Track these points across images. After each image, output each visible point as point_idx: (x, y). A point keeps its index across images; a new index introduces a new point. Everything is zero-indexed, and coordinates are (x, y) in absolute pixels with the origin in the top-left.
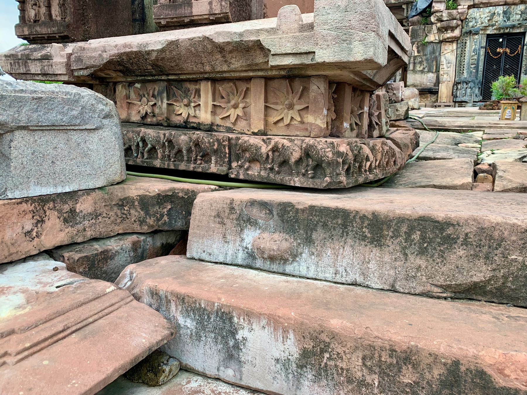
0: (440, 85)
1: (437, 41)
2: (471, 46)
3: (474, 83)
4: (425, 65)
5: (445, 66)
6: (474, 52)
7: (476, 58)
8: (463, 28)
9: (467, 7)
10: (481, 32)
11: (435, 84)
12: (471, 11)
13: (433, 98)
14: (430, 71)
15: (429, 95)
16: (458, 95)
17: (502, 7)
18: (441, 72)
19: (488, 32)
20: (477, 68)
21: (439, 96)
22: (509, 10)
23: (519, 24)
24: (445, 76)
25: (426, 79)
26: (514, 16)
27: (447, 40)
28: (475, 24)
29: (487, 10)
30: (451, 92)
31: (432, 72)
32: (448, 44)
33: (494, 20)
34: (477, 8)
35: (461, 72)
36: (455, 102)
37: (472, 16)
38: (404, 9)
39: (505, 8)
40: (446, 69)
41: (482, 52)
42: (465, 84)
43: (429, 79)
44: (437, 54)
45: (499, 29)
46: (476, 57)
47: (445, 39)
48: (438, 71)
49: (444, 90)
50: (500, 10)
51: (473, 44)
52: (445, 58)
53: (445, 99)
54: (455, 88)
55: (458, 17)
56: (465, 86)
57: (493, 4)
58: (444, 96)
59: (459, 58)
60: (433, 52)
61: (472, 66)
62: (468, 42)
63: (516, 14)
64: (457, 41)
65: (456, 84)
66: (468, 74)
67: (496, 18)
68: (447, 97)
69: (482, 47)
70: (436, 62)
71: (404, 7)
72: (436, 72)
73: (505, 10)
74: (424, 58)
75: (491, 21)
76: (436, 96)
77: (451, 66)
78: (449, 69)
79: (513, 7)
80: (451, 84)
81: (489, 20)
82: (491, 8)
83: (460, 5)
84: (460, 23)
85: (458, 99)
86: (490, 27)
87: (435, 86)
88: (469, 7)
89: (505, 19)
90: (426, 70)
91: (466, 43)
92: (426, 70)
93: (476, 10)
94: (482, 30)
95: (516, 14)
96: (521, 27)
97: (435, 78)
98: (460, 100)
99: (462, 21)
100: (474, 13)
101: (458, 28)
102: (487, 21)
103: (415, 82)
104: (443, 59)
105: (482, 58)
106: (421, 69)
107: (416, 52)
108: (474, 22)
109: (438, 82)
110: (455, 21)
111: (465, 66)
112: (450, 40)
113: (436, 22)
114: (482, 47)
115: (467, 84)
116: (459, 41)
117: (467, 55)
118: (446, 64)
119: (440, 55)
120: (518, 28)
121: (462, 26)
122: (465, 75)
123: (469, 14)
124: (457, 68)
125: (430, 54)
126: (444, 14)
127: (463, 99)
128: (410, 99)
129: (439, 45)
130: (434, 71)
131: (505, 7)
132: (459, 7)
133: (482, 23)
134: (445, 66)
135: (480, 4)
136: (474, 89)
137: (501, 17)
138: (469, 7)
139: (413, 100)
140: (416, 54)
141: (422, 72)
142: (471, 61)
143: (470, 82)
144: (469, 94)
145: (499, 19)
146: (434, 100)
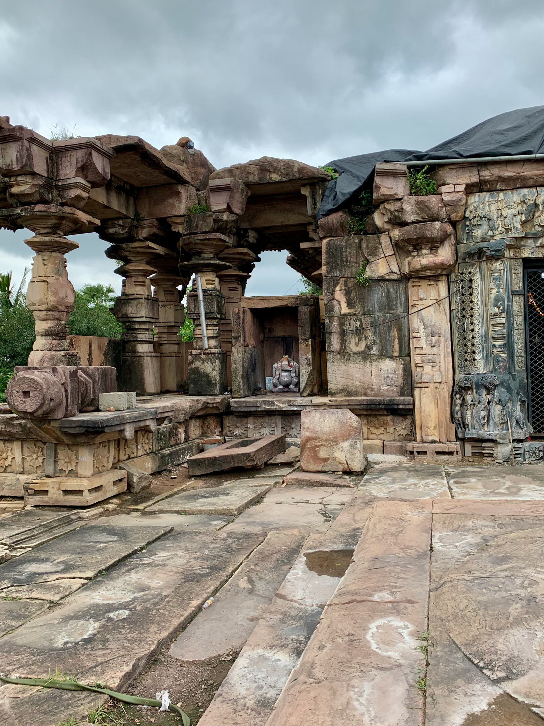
0: (417, 392)
1: (395, 277)
2: (486, 291)
3: (509, 390)
4: (370, 337)
5: (423, 342)
6: (496, 306)
7: (504, 321)
8: (458, 242)
9: (462, 188)
10: (507, 254)
11: (402, 388)
12: (474, 199)
13: (401, 427)
14: (384, 354)
15: (389, 418)
16: (469, 420)
18: (416, 359)
19: (526, 253)
20: (509, 347)
21: (417, 423)
24: (428, 368)
25: (378, 376)
27: (422, 274)
28: (490, 233)
29: (515, 197)
30: (448, 412)
31: (392, 358)
32: (424, 283)
34: (488, 191)
35: (469, 358)
36: (463, 440)
37: (480, 212)
38: (305, 197)
40: (426, 349)
41: (517, 305)
42: (484, 392)
43: (384, 374)
44: (400, 310)
46: (503, 320)
47: (417, 271)
48: (405, 354)
49: (430, 408)
51: (492, 285)
52: (422, 321)
53: (436, 432)
54: (459, 402)
55: (443, 213)
56: (485, 397)
57: (531, 182)
58: (432, 422)
59: (456, 322)
60: (389, 305)
61: (497, 343)
62: (477, 278)
64: (448, 276)
65: (459, 390)
66: (487, 363)
68: (439, 426)
69: (514, 293)
70: (400, 330)
71: (305, 192)
72: (400, 356)
74: (366, 320)
75: (529, 225)
76: (409, 421)
77: (439, 341)
78: (435, 350)
80: (445, 391)
82: (525, 191)
83: (444, 184)
84: (449, 228)
85: (471, 434)
86: (530, 241)
87: (402, 394)
88: (470, 189)
90: (375, 350)
91: (471, 281)
92: (375, 350)
93: (486, 196)
94: (509, 247)
97: (401, 372)
98: (475, 437)
99: (454, 224)
100: (482, 204)
101: (447, 244)
103: (350, 382)
104: (415, 322)
105: (519, 320)
106: (362, 347)
107: (344, 305)
108: (485, 227)
109: (409, 385)
110: (437, 225)
111: (477, 342)
112: (429, 273)
113: (387, 226)
114: (514, 293)
115: (489, 391)
116: (453, 277)
117: (478, 312)
118: (427, 336)
119: (406, 311)
121: (456, 237)
122: (481, 366)
123: (471, 208)
124: (456, 348)
125: (380, 310)
126: (407, 207)
127: (486, 432)
128: (336, 441)
129: (402, 287)
130: (396, 354)
132: (444, 189)
133: (508, 230)
134: (423, 342)
135: (497, 182)
136: (509, 405)
139: (346, 445)
140: (345, 310)
141: (365, 356)
142: (491, 328)
143: (496, 386)
144: (497, 420)
146: (403, 432)
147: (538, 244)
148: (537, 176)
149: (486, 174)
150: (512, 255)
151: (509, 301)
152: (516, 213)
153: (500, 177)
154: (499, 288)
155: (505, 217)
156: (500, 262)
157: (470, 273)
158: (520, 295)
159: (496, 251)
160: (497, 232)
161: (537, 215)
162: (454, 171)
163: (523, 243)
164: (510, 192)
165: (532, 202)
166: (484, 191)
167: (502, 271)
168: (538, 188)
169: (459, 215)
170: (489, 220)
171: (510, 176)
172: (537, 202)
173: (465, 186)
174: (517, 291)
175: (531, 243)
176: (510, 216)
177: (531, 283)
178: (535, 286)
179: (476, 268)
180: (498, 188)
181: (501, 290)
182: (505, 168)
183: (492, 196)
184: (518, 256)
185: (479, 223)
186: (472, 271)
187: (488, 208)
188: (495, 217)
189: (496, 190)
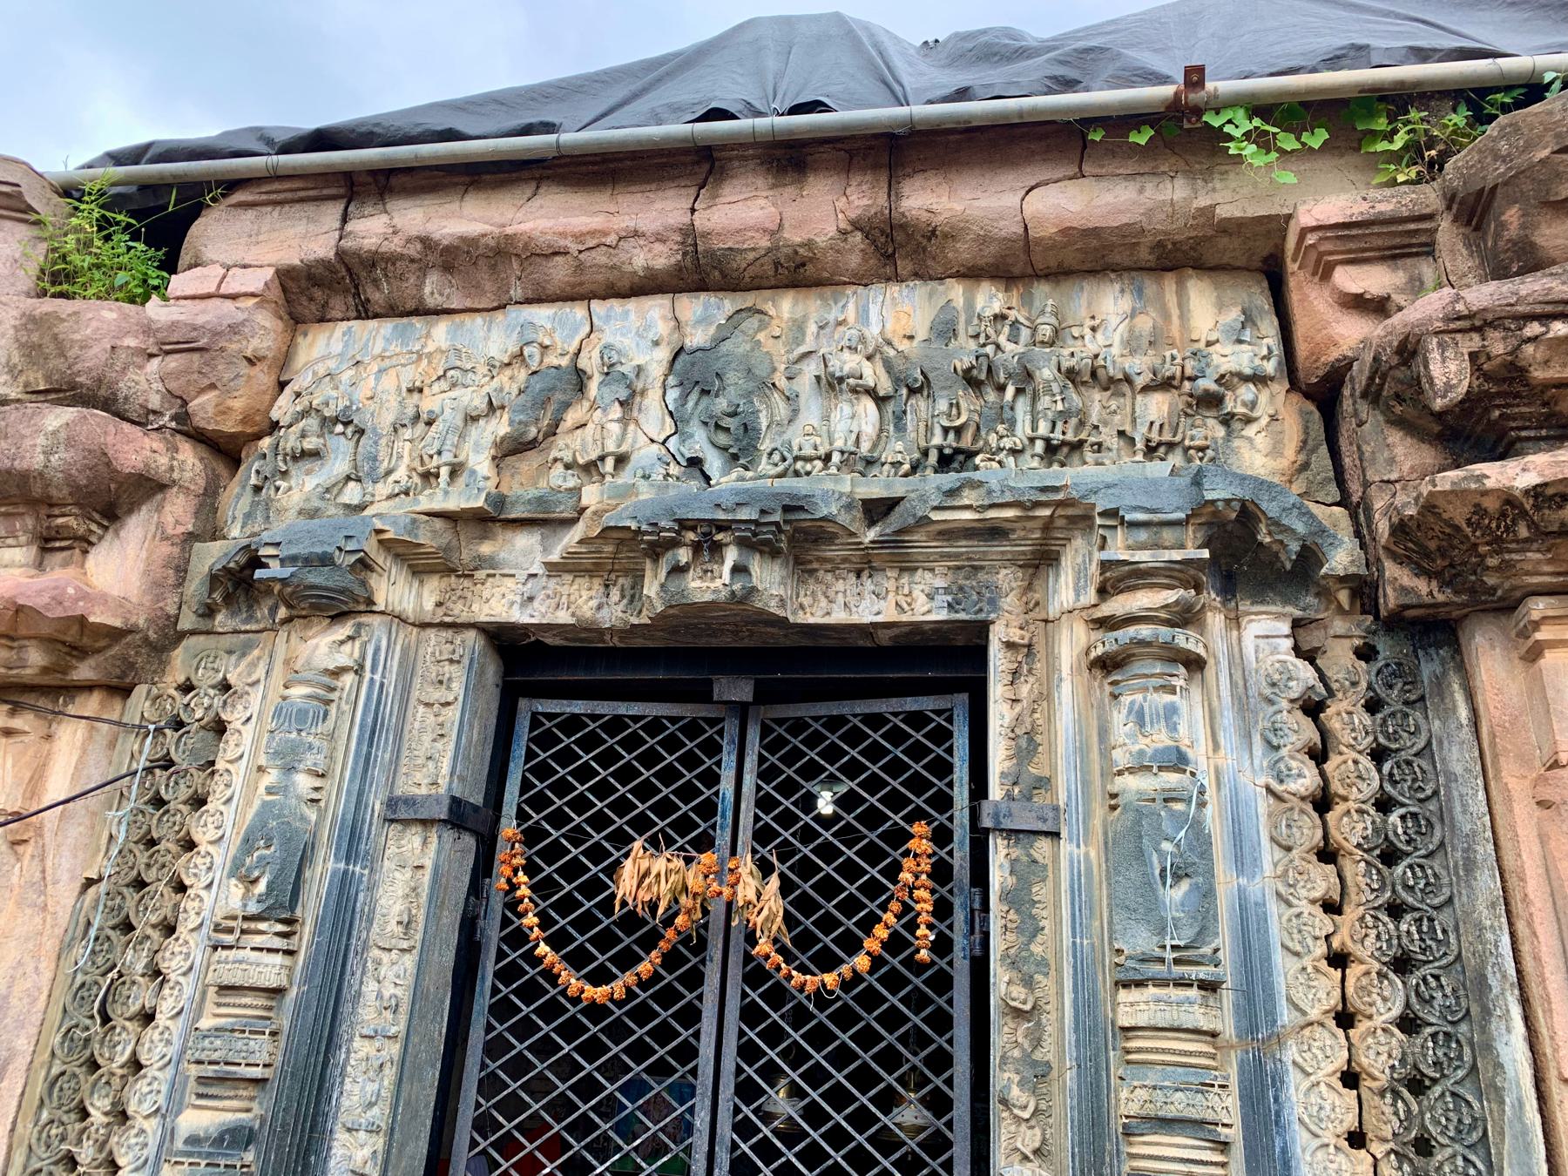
10: (394, 590)
17: (655, 309)
22: (737, 346)
23: (877, 510)
26: (811, 413)
29: (492, 337)
33: (568, 445)
34: (394, 311)
37: (331, 398)
39: (701, 316)
41: (408, 880)
45: (624, 551)
50: (639, 333)
57: (559, 272)
63: (832, 384)
67: (592, 429)
69: (401, 813)
73: (697, 338)
75: (527, 464)
79: (785, 306)
81: (512, 449)
82: (542, 314)
86: (525, 541)
88: (310, 294)
89: (699, 442)
91: (219, 728)
93: (377, 334)
94: (417, 562)
95: (832, 384)
96: (895, 555)
100: (349, 361)
102: (481, 463)
105: (392, 981)
114: (401, 813)
120: (865, 565)
131: (692, 306)
137: (653, 418)
138: (310, 294)
145: (638, 455)
147: (555, 557)
148: (579, 237)
149: (373, 229)
150: (429, 605)
151: (350, 855)
152: (480, 403)
153: (426, 242)
154: (290, 769)
155: (429, 423)
156: (345, 630)
157: (225, 687)
158: (426, 823)
159: (309, 561)
160: (383, 489)
161: (571, 417)
162: (251, 214)
163: (486, 548)
165: (564, 362)
166: (376, 316)
167: (348, 679)
168: (595, 304)
169: (238, 404)
170: (361, 432)
171: (463, 239)
172: (583, 363)
173: (270, 272)
174: (410, 802)
175: (527, 553)
176: (450, 418)
177: (542, 771)
178: (562, 788)
179: (253, 665)
180: (431, 302)
181: (303, 782)
182: (455, 206)
183: (402, 335)
184: (460, 612)
185: (310, 443)
187: (371, 381)
188: (387, 419)
189: (421, 311)
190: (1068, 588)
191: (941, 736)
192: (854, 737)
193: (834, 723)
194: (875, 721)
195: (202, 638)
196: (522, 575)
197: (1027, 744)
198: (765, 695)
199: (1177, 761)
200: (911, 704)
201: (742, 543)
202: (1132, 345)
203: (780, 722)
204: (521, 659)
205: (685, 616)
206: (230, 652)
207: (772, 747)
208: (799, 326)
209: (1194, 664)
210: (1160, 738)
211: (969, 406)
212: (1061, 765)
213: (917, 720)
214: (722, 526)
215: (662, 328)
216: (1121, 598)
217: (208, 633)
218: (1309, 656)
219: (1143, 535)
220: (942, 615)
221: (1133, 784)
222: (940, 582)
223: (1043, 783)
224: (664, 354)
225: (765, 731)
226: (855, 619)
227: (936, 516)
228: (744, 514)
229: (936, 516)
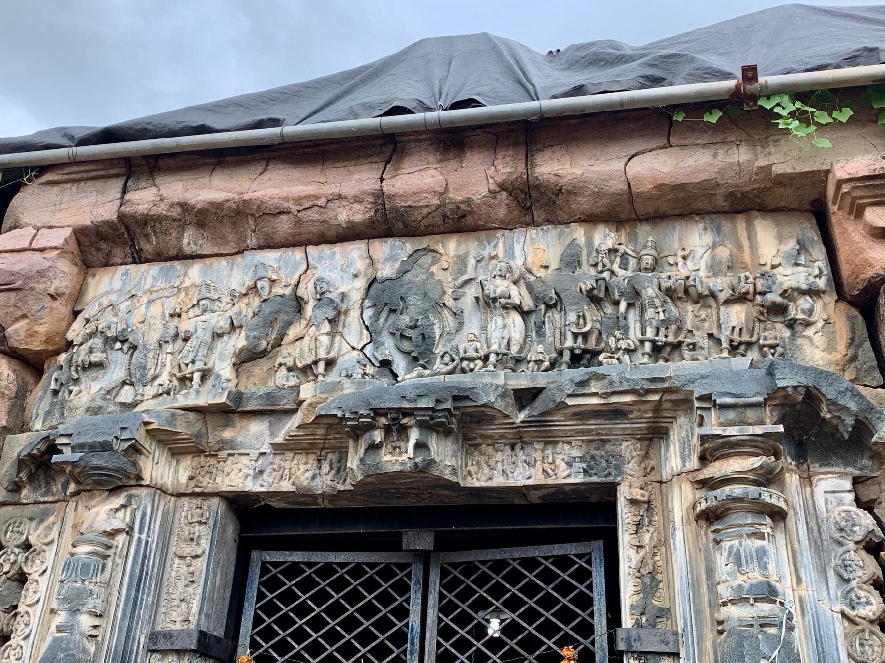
10: (158, 468)
12: (107, 284)
17: (355, 251)
19: (237, 476)
22: (416, 276)
23: (525, 397)
26: (472, 325)
29: (234, 275)
33: (289, 353)
34: (160, 257)
37: (112, 323)
39: (388, 255)
45: (331, 434)
50: (343, 269)
57: (283, 226)
63: (487, 303)
67: (307, 341)
73: (386, 271)
75: (259, 368)
79: (451, 247)
81: (247, 358)
82: (271, 257)
88: (97, 247)
89: (389, 349)
91: (22, 579)
94: (174, 445)
95: (487, 303)
96: (541, 432)
100: (126, 294)
102: (224, 369)
120: (517, 440)
131: (381, 248)
135: (181, 225)
137: (354, 331)
138: (97, 247)
145: (342, 359)
147: (279, 439)
148: (298, 201)
149: (145, 198)
150: (183, 478)
152: (224, 324)
153: (185, 207)
154: (74, 612)
155: (186, 340)
156: (118, 501)
157: (27, 546)
158: (180, 653)
160: (150, 391)
161: (293, 332)
162: (56, 189)
163: (227, 434)
164: (223, 263)
165: (287, 291)
166: (147, 261)
167: (121, 539)
168: (311, 249)
169: (42, 329)
170: (134, 348)
171: (212, 204)
172: (301, 292)
173: (68, 232)
174: (168, 635)
175: (258, 436)
176: (202, 335)
177: (270, 609)
178: (285, 622)
179: (49, 528)
180: (188, 250)
181: (85, 622)
182: (206, 180)
184: (207, 484)
185: (95, 358)
186: (33, 539)
187: (143, 310)
188: (154, 337)
189: (182, 257)
190: (676, 456)
191: (584, 575)
192: (514, 577)
193: (498, 566)
194: (530, 564)
195: (10, 508)
196: (254, 454)
197: (651, 582)
198: (443, 544)
199: (769, 593)
200: (559, 550)
201: (423, 426)
202: (715, 269)
203: (455, 566)
204: (254, 520)
205: (379, 484)
206: (31, 519)
207: (449, 587)
208: (462, 261)
209: (778, 515)
210: (755, 576)
211: (592, 318)
212: (678, 598)
213: (563, 562)
214: (407, 413)
215: (360, 265)
216: (717, 464)
217: (15, 504)
218: (868, 506)
219: (731, 415)
220: (579, 479)
221: (734, 612)
222: (576, 453)
223: (665, 613)
224: (361, 284)
225: (444, 573)
226: (511, 483)
227: (570, 402)
228: (423, 403)
229: (570, 402)
